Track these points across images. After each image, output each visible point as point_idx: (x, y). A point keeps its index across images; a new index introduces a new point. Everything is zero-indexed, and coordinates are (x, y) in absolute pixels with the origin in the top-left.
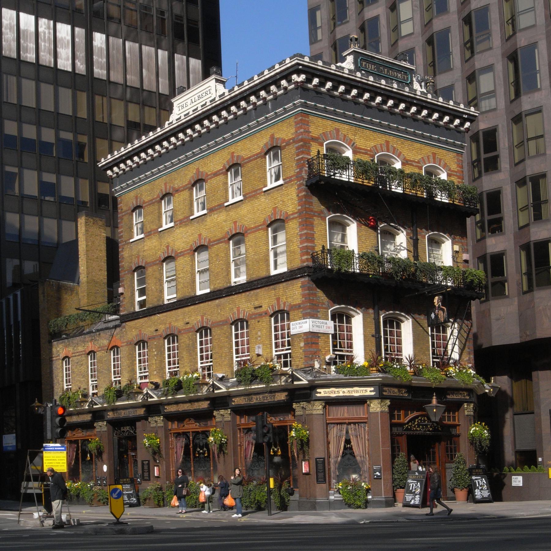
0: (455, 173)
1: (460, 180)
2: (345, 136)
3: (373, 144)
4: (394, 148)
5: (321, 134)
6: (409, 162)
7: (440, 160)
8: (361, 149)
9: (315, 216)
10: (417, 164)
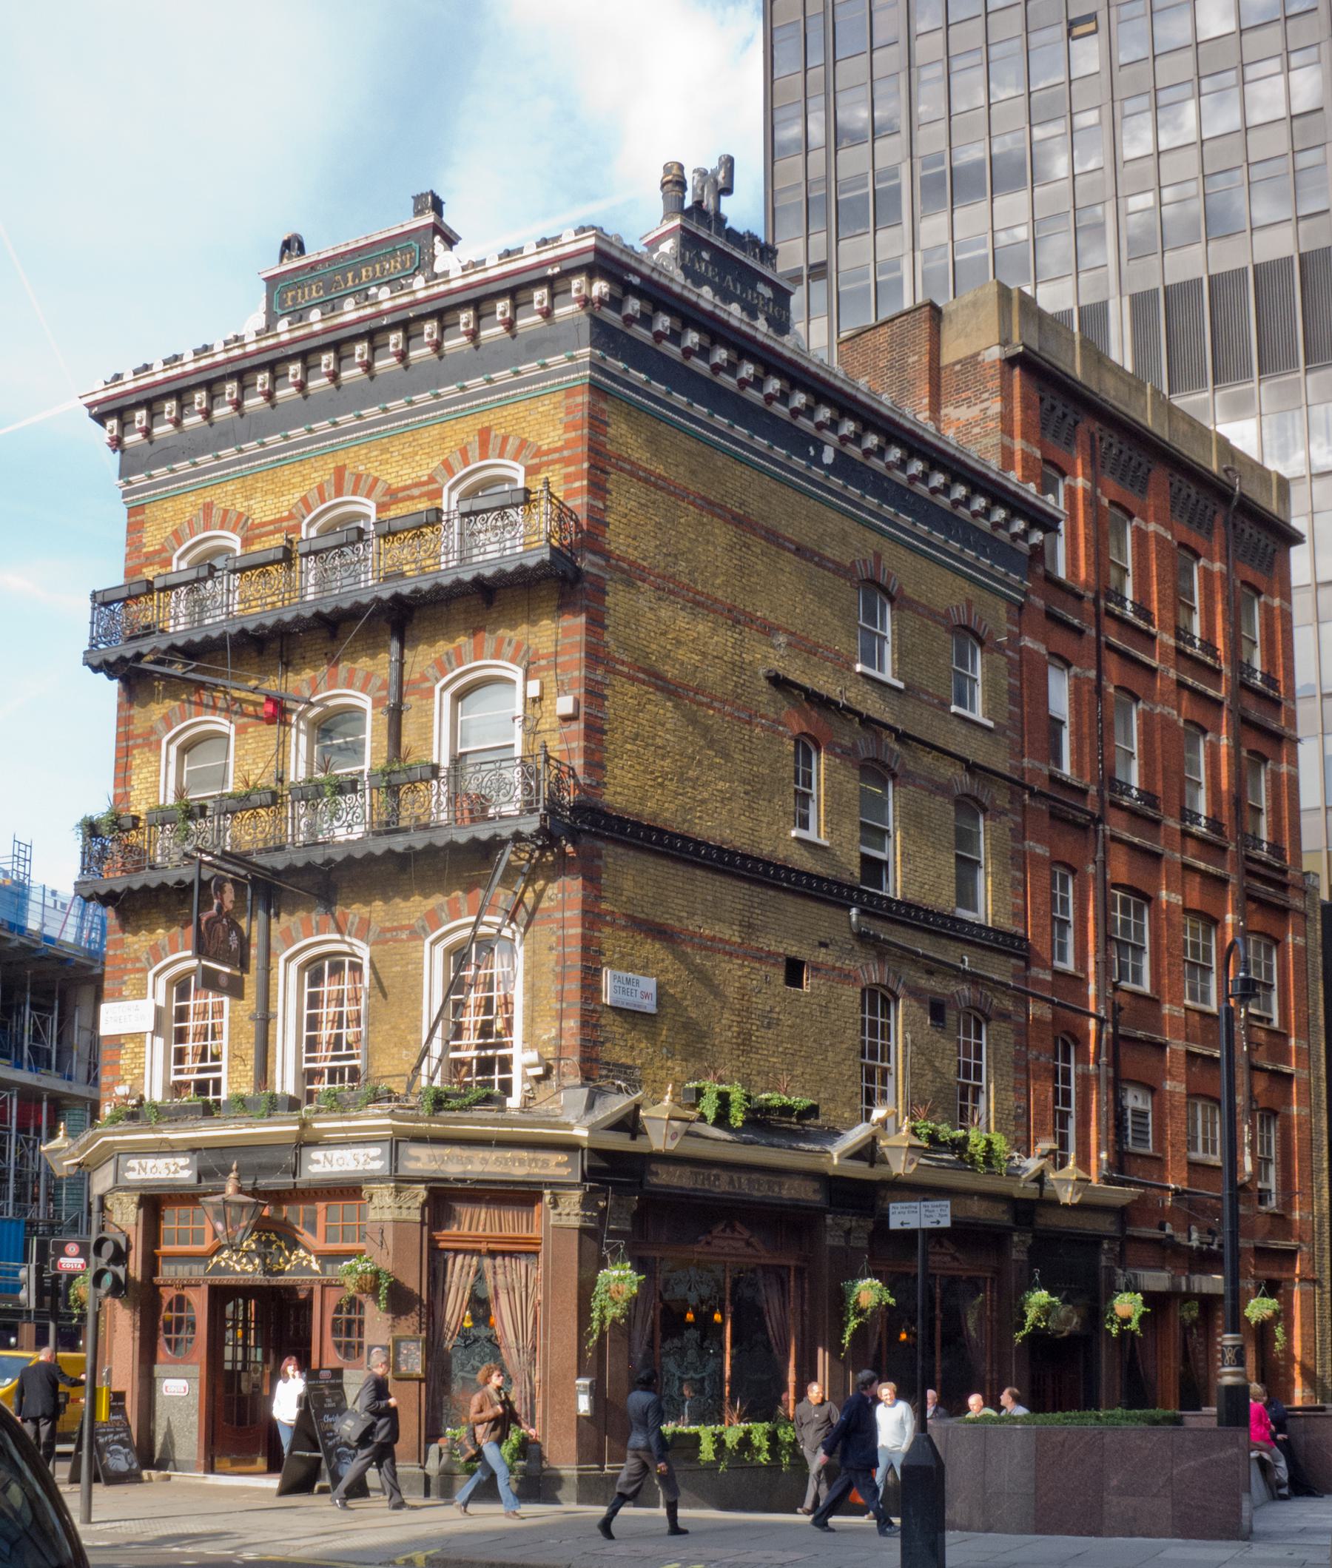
0: (556, 456)
1: (571, 469)
2: (226, 512)
3: (298, 496)
4: (358, 477)
5: (167, 538)
6: (401, 495)
7: (505, 439)
8: (263, 524)
9: (137, 746)
10: (425, 489)
